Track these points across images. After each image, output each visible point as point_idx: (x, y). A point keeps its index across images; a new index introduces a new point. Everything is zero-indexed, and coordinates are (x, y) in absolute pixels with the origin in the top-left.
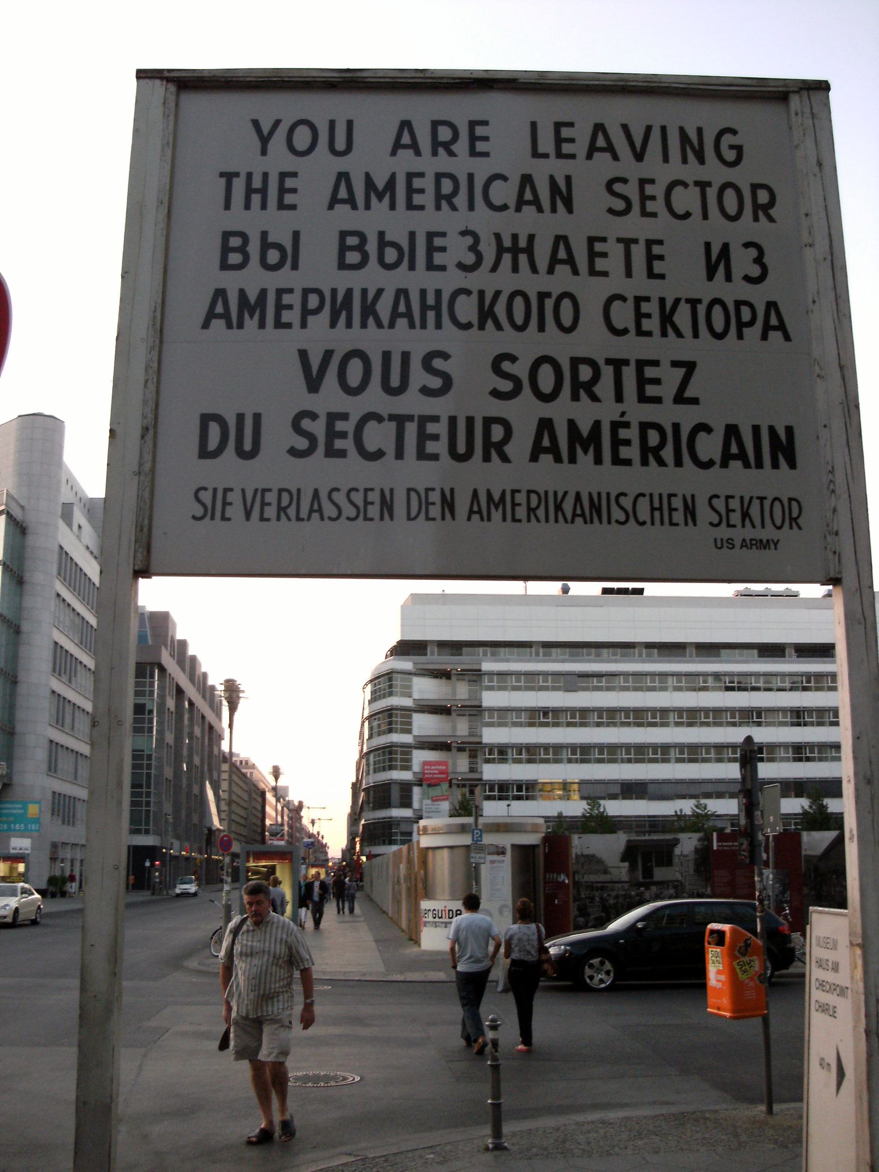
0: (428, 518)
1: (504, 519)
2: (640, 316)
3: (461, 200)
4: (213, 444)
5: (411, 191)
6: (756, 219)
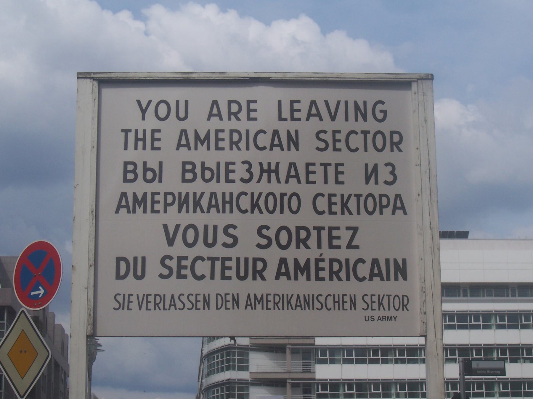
0: (226, 308)
1: (263, 309)
2: (331, 204)
3: (243, 145)
4: (123, 272)
5: (218, 140)
6: (392, 150)
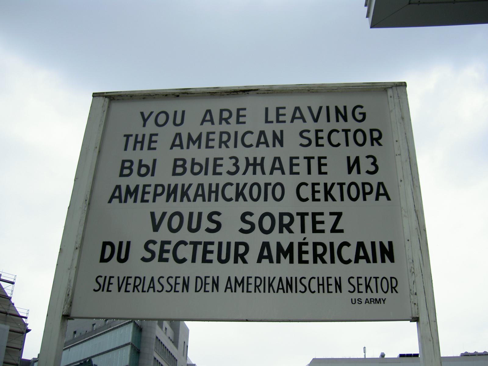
0: (205, 291)
1: (243, 291)
2: (314, 192)
3: (231, 143)
4: (107, 256)
5: (208, 140)
6: (372, 144)
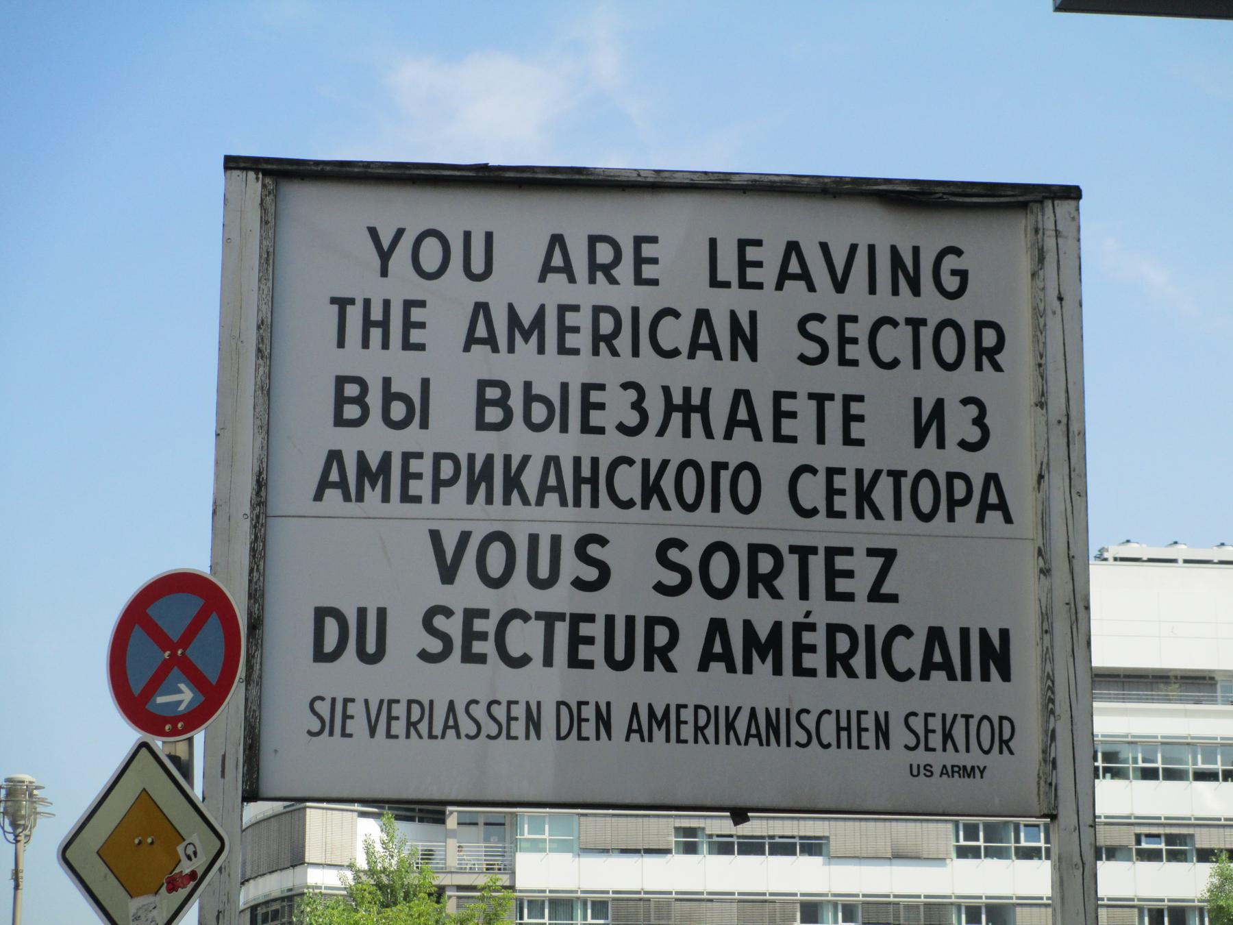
0: (580, 738)
1: (668, 740)
4: (330, 644)
6: (979, 367)
